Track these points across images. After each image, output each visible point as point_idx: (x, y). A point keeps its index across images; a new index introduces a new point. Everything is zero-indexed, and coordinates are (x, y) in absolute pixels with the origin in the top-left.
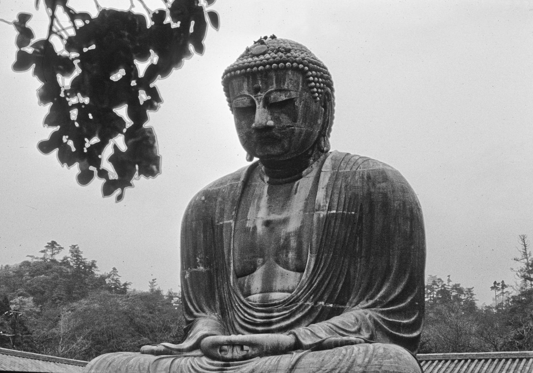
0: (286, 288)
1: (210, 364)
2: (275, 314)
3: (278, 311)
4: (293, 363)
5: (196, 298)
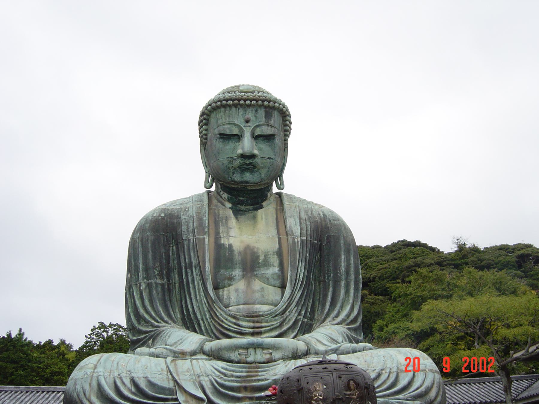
0: (270, 302)
1: (232, 366)
2: (264, 324)
3: (266, 322)
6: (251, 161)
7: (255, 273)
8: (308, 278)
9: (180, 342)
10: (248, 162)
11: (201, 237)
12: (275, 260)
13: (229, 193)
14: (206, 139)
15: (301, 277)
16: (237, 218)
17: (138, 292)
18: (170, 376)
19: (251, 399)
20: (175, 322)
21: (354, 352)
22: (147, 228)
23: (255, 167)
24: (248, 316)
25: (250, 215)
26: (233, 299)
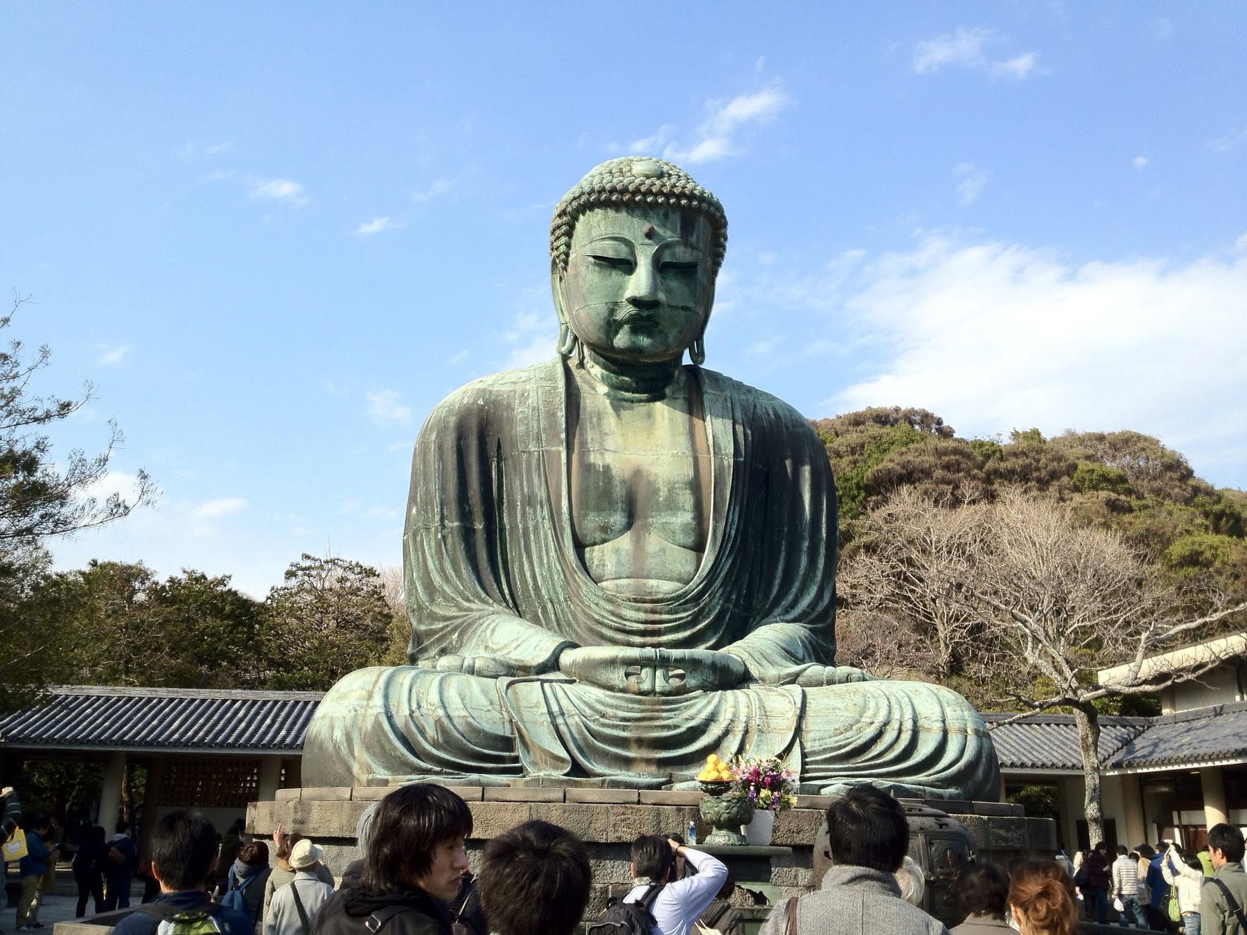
0: (675, 575)
3: (669, 613)
4: (799, 705)
5: (459, 577)
6: (651, 312)
7: (650, 520)
8: (742, 532)
9: (514, 645)
10: (645, 313)
11: (554, 449)
12: (687, 499)
13: (605, 367)
14: (566, 262)
15: (733, 532)
16: (618, 416)
17: (433, 543)
18: (505, 714)
19: (648, 761)
20: (499, 603)
21: (831, 682)
22: (452, 425)
23: (657, 324)
24: (636, 601)
25: (642, 409)
26: (610, 567)
